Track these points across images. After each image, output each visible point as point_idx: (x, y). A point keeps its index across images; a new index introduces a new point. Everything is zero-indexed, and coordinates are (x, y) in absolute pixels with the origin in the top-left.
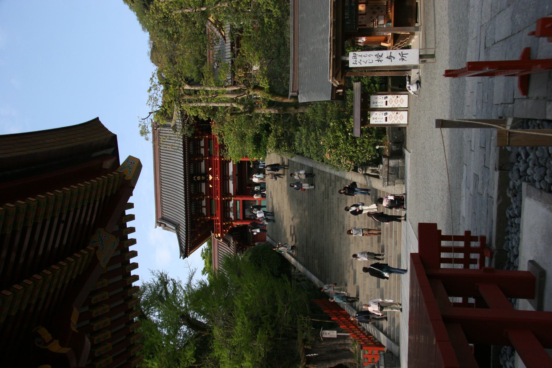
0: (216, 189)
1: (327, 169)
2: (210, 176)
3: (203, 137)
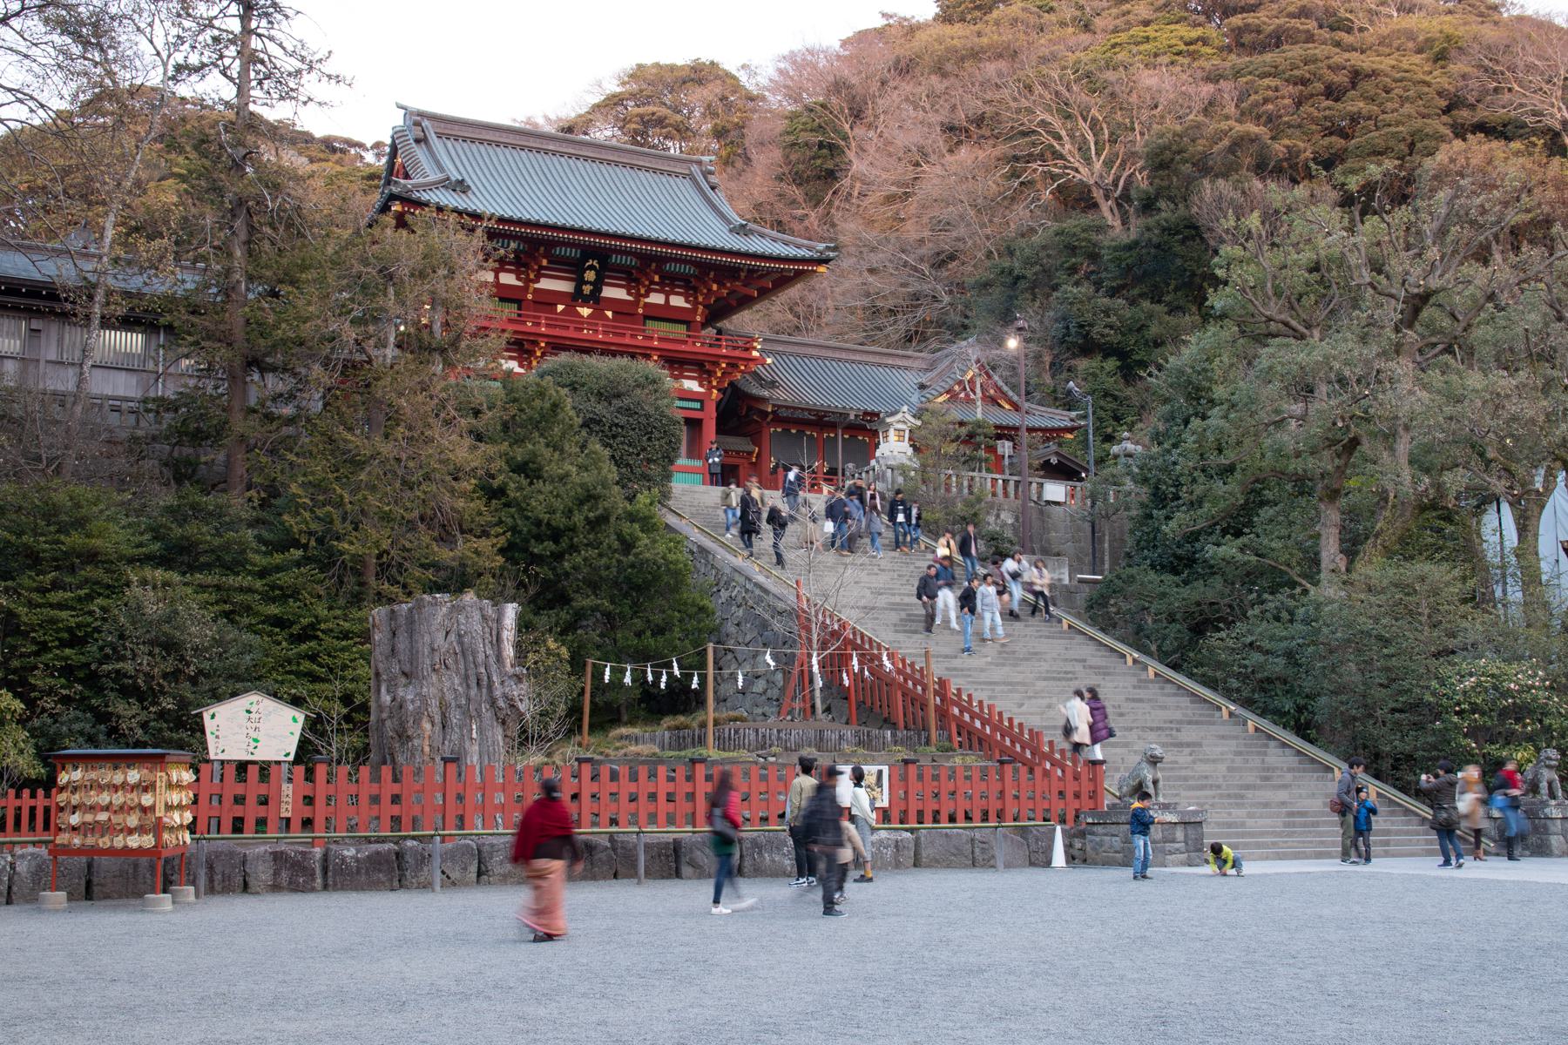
0: (572, 326)
2: (590, 311)
3: (701, 307)
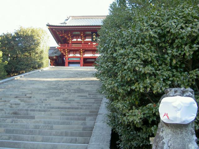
1: (109, 80)
